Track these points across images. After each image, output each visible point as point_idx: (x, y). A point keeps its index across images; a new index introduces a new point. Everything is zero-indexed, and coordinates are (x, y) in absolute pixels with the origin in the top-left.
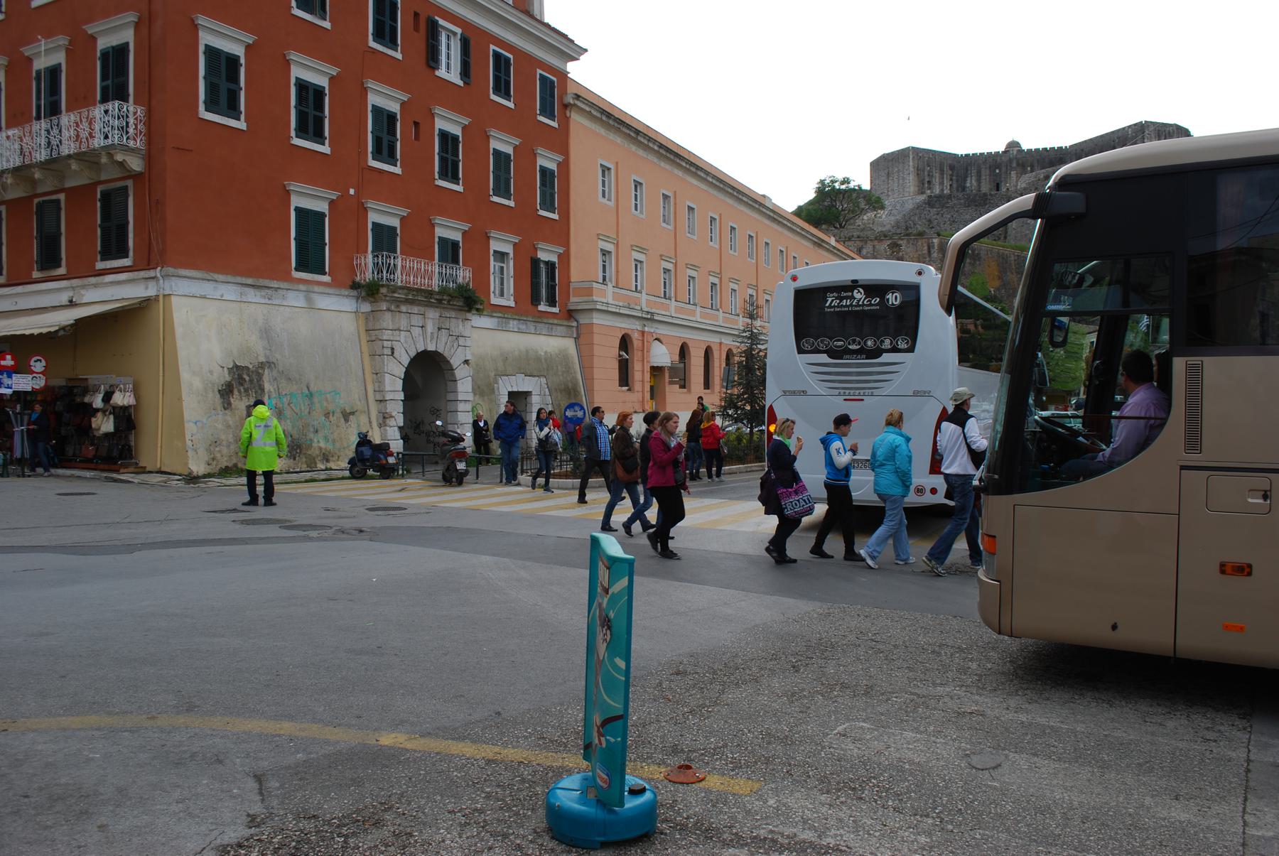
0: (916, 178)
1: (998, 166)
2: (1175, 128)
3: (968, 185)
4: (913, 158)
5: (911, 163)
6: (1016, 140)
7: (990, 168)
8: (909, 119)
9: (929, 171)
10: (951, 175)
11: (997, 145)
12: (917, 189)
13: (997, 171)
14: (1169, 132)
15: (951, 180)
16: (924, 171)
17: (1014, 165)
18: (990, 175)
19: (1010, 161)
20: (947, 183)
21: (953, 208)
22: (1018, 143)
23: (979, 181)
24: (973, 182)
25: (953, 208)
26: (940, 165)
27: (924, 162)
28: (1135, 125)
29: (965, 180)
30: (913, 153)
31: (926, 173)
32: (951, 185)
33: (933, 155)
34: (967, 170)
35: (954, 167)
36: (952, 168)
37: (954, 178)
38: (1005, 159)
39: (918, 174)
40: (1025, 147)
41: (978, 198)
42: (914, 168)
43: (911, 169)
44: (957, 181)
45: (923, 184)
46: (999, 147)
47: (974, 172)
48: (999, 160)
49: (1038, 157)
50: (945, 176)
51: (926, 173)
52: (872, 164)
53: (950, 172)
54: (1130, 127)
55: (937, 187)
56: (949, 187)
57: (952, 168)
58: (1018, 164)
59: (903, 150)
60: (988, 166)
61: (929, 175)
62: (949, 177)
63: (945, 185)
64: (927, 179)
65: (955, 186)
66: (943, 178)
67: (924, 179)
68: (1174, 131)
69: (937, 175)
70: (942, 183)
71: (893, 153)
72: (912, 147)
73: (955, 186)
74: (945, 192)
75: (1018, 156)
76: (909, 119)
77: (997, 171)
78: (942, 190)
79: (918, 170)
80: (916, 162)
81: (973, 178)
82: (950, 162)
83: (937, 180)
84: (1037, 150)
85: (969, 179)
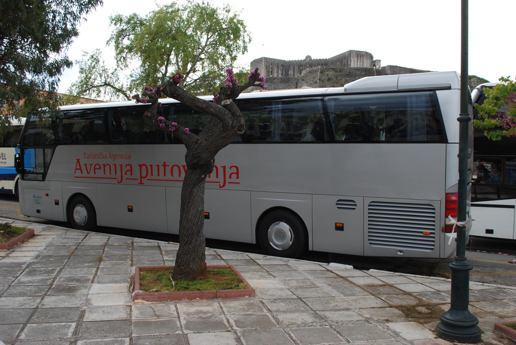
0: (266, 70)
1: (302, 66)
2: (365, 53)
3: (290, 73)
4: (264, 62)
5: (263, 64)
6: (309, 55)
7: (298, 66)
8: (263, 45)
9: (272, 67)
10: (282, 69)
11: (301, 57)
12: (266, 74)
13: (301, 68)
14: (362, 55)
15: (282, 71)
16: (269, 67)
17: (308, 65)
18: (298, 69)
19: (306, 64)
20: (280, 72)
21: (275, 83)
22: (310, 56)
23: (294, 71)
24: (292, 72)
25: (275, 83)
26: (277, 65)
27: (269, 63)
28: (348, 51)
29: (288, 71)
30: (264, 60)
31: (270, 68)
32: (282, 73)
33: (274, 60)
34: (289, 67)
35: (284, 65)
36: (283, 66)
37: (284, 70)
38: (304, 63)
39: (266, 68)
40: (313, 58)
41: (286, 79)
42: (265, 66)
43: (263, 66)
44: (285, 71)
45: (269, 72)
46: (303, 58)
47: (292, 68)
48: (302, 63)
49: (317, 63)
50: (279, 69)
51: (270, 68)
52: (251, 63)
53: (282, 68)
54: (347, 52)
55: (276, 74)
56: (281, 74)
57: (283, 66)
58: (309, 65)
59: (261, 58)
60: (297, 66)
61: (272, 69)
62: (281, 70)
63: (279, 73)
64: (271, 70)
65: (284, 73)
66: (278, 70)
67: (269, 71)
68: (364, 54)
69: (276, 69)
70: (278, 72)
71: (258, 59)
72: (264, 57)
73: (284, 73)
74: (279, 76)
75: (310, 62)
76: (263, 45)
77: (301, 68)
78: (278, 75)
79: (266, 67)
80: (266, 63)
81: (292, 70)
82: (282, 63)
83: (275, 71)
84: (317, 60)
85: (290, 71)
